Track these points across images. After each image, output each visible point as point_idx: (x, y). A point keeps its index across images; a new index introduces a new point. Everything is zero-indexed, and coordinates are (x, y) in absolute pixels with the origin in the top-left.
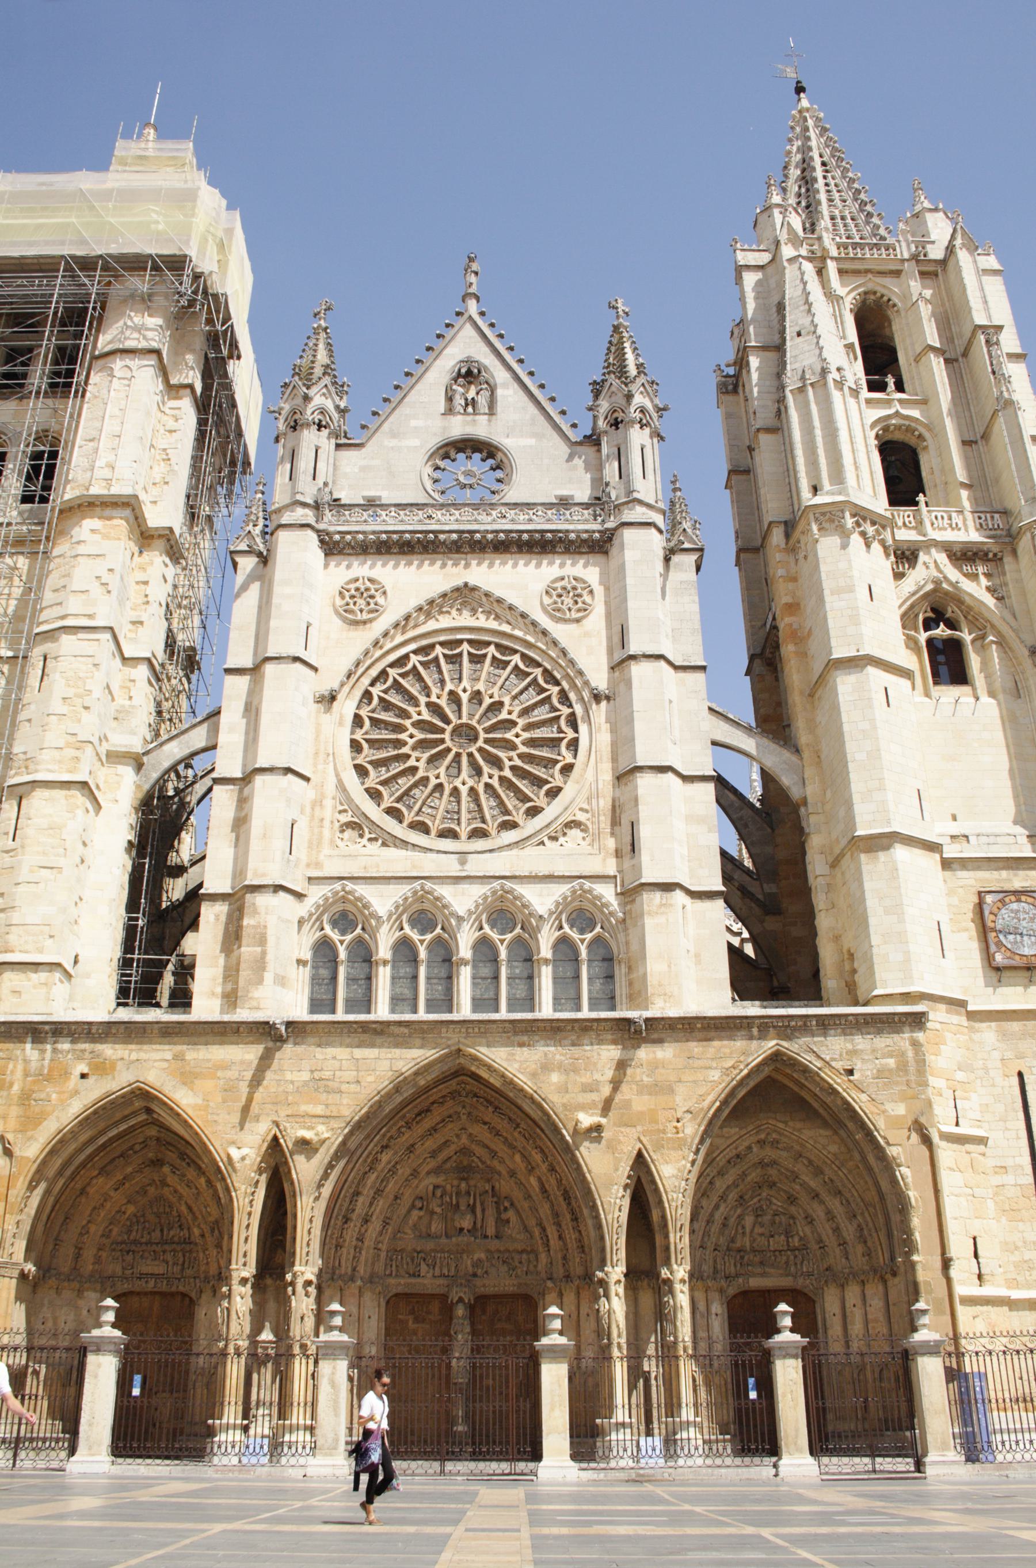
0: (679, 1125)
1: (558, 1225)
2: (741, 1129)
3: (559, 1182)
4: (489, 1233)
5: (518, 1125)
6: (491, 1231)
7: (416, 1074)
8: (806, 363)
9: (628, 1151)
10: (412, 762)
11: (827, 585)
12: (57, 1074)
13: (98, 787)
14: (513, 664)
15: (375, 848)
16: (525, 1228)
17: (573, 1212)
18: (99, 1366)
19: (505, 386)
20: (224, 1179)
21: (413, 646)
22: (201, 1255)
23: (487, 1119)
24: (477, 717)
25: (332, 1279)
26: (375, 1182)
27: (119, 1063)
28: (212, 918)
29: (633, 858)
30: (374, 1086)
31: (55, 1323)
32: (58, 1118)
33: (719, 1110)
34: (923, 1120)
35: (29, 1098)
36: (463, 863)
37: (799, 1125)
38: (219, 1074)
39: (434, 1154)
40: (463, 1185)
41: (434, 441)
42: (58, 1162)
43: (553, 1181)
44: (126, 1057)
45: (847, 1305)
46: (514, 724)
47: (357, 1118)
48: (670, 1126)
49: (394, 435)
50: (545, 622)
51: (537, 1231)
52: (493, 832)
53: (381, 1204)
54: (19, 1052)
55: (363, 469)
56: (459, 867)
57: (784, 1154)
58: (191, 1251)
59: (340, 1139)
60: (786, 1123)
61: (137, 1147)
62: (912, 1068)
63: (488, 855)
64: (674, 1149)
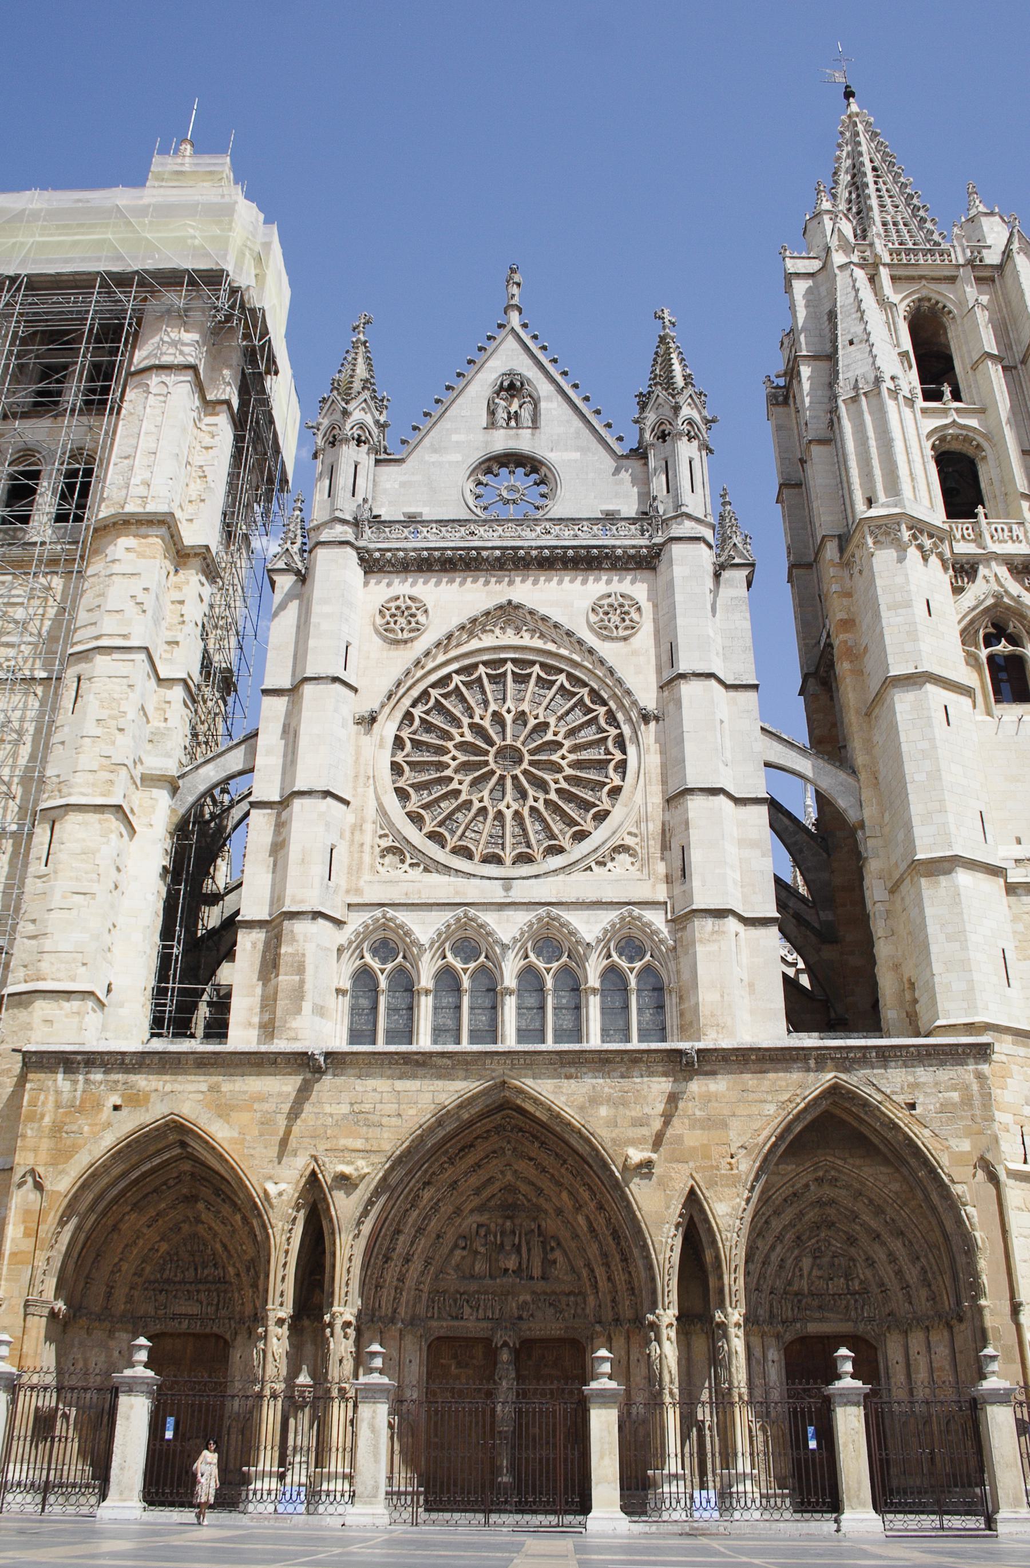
0: (733, 1161)
1: (607, 1265)
2: (798, 1166)
3: (608, 1220)
5: (565, 1161)
6: (537, 1272)
7: (460, 1106)
8: (859, 372)
9: (680, 1187)
10: (454, 785)
11: (883, 600)
12: (89, 1106)
13: (132, 811)
14: (558, 683)
15: (416, 873)
16: (573, 1269)
17: (622, 1252)
18: (131, 1407)
19: (549, 399)
20: (260, 1215)
21: (455, 666)
22: (236, 1295)
23: (533, 1155)
24: (522, 739)
25: (372, 1321)
26: (416, 1221)
27: (153, 1095)
28: (249, 945)
29: (684, 883)
30: (416, 1119)
31: (86, 1364)
32: (90, 1151)
33: (775, 1145)
34: (989, 1157)
35: (60, 1130)
36: (507, 889)
37: (858, 1162)
38: (256, 1106)
39: (477, 1191)
40: (508, 1223)
41: (476, 456)
42: (90, 1197)
43: (602, 1221)
44: (160, 1088)
45: (911, 1353)
46: (560, 745)
48: (724, 1163)
49: (435, 450)
50: (591, 640)
51: (585, 1273)
52: (539, 857)
53: (423, 1243)
54: (50, 1083)
55: (403, 484)
56: (504, 894)
57: (844, 1192)
58: (225, 1291)
59: (381, 1174)
60: (844, 1160)
61: (171, 1182)
62: (977, 1103)
63: (533, 881)
64: (727, 1186)
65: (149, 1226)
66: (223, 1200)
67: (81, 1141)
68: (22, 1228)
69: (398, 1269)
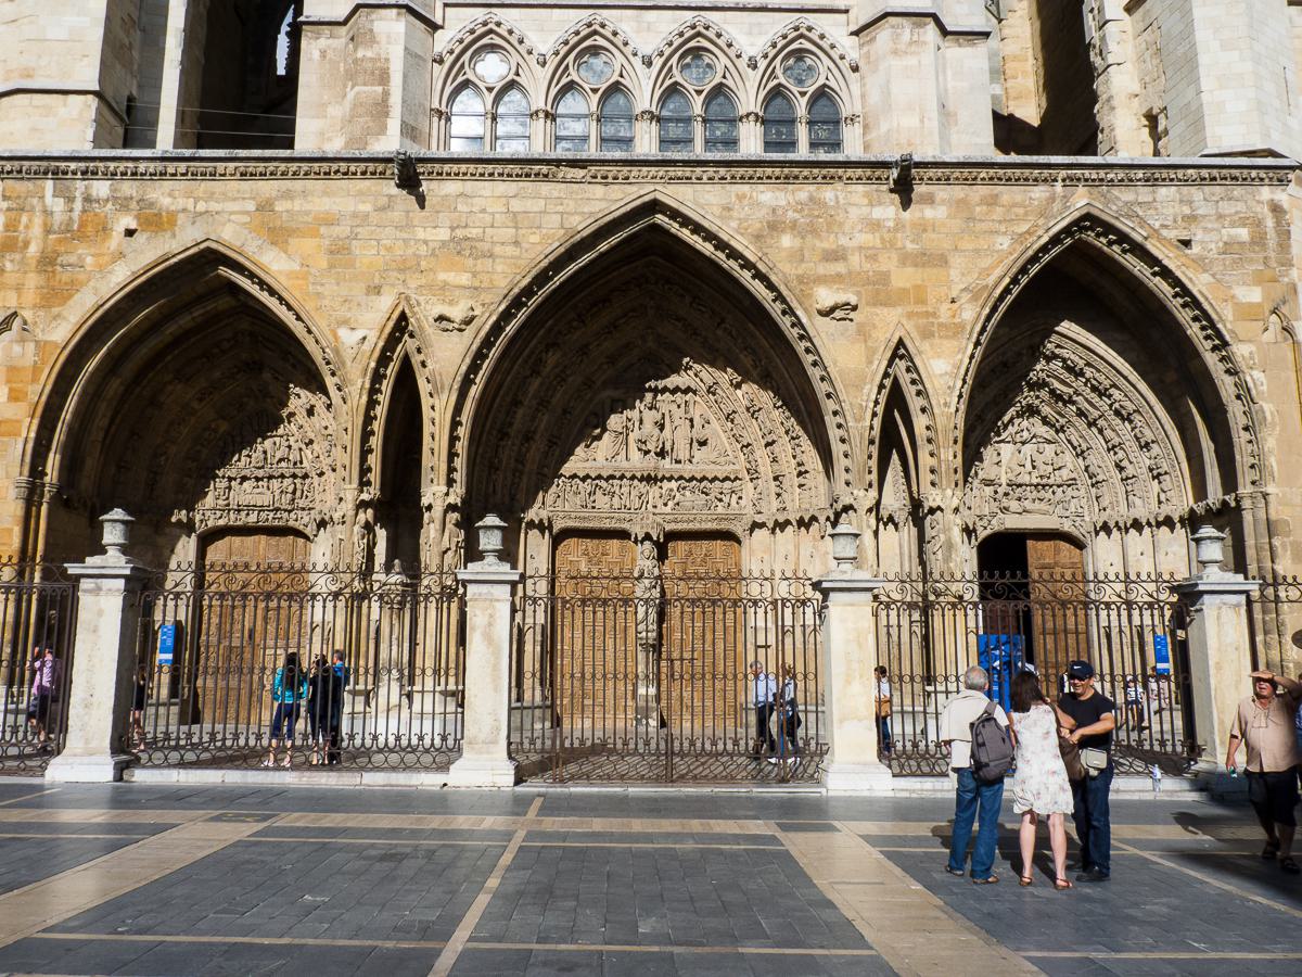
0: (955, 306)
4: (681, 457)
12: (90, 228)
18: (100, 613)
27: (181, 216)
28: (316, 55)
30: (540, 248)
33: (1007, 291)
35: (52, 263)
38: (323, 230)
39: (612, 360)
44: (190, 207)
47: (516, 290)
53: (545, 420)
54: (35, 201)
59: (494, 318)
62: (1272, 241)
64: (947, 337)
65: (201, 400)
66: (294, 366)
67: (82, 277)
68: (6, 390)
69: (515, 448)
